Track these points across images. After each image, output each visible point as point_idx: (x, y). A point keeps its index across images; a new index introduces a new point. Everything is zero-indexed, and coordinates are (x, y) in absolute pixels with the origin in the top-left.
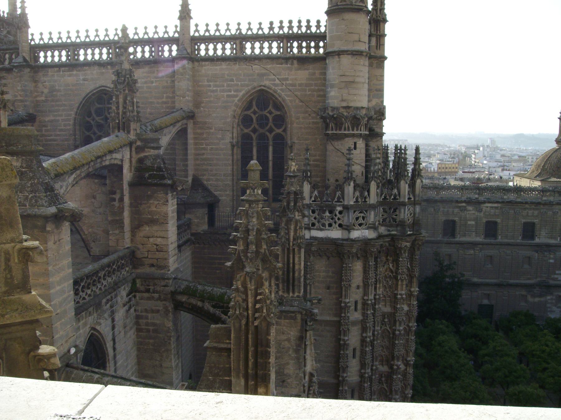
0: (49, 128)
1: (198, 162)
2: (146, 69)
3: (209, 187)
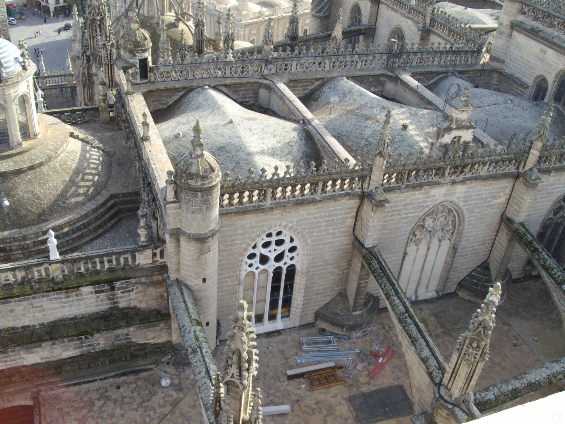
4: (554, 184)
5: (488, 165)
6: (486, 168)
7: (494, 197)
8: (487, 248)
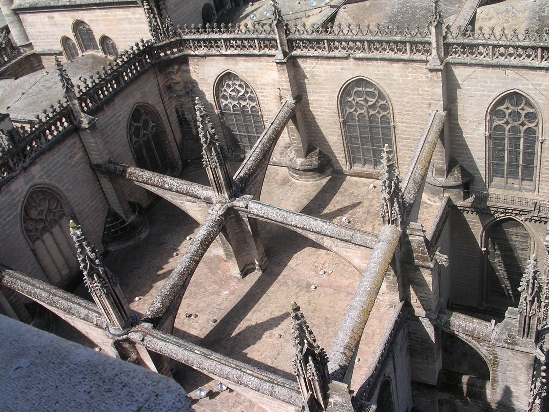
0: (314, 105)
1: (454, 146)
2: (401, 65)
3: (465, 166)
4: (114, 115)
5: (43, 136)
6: (43, 140)
7: (71, 157)
8: (101, 198)
